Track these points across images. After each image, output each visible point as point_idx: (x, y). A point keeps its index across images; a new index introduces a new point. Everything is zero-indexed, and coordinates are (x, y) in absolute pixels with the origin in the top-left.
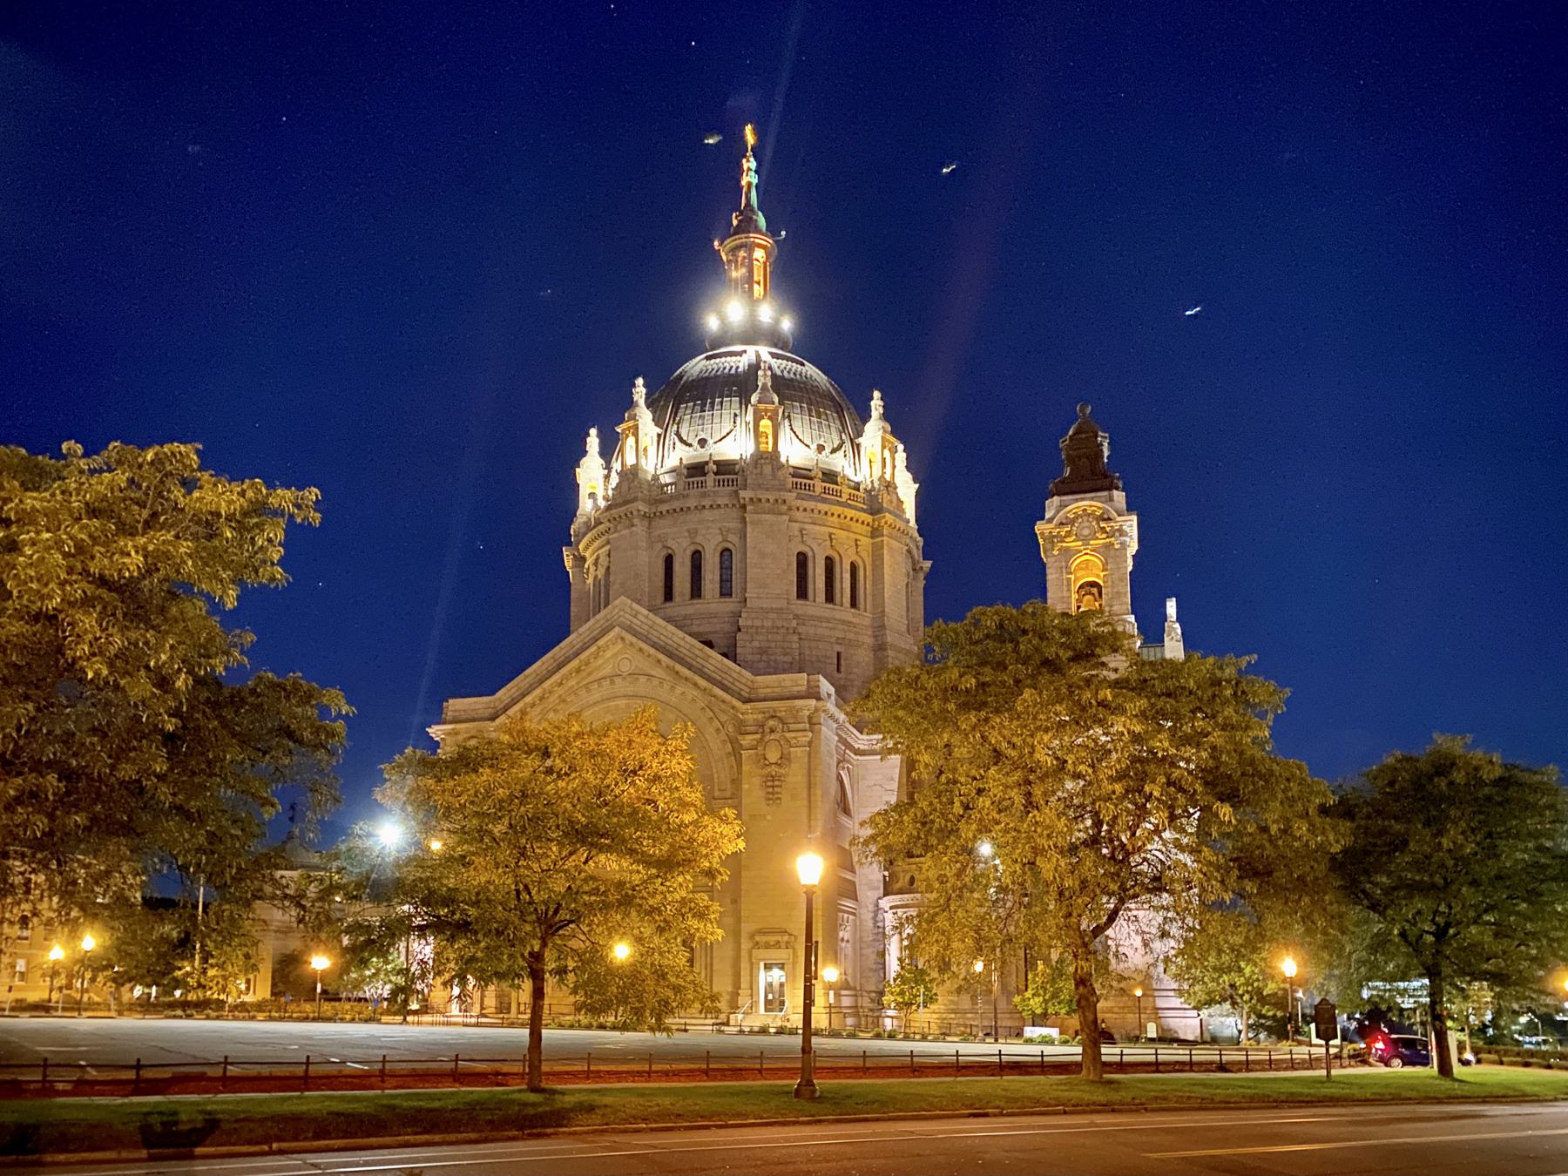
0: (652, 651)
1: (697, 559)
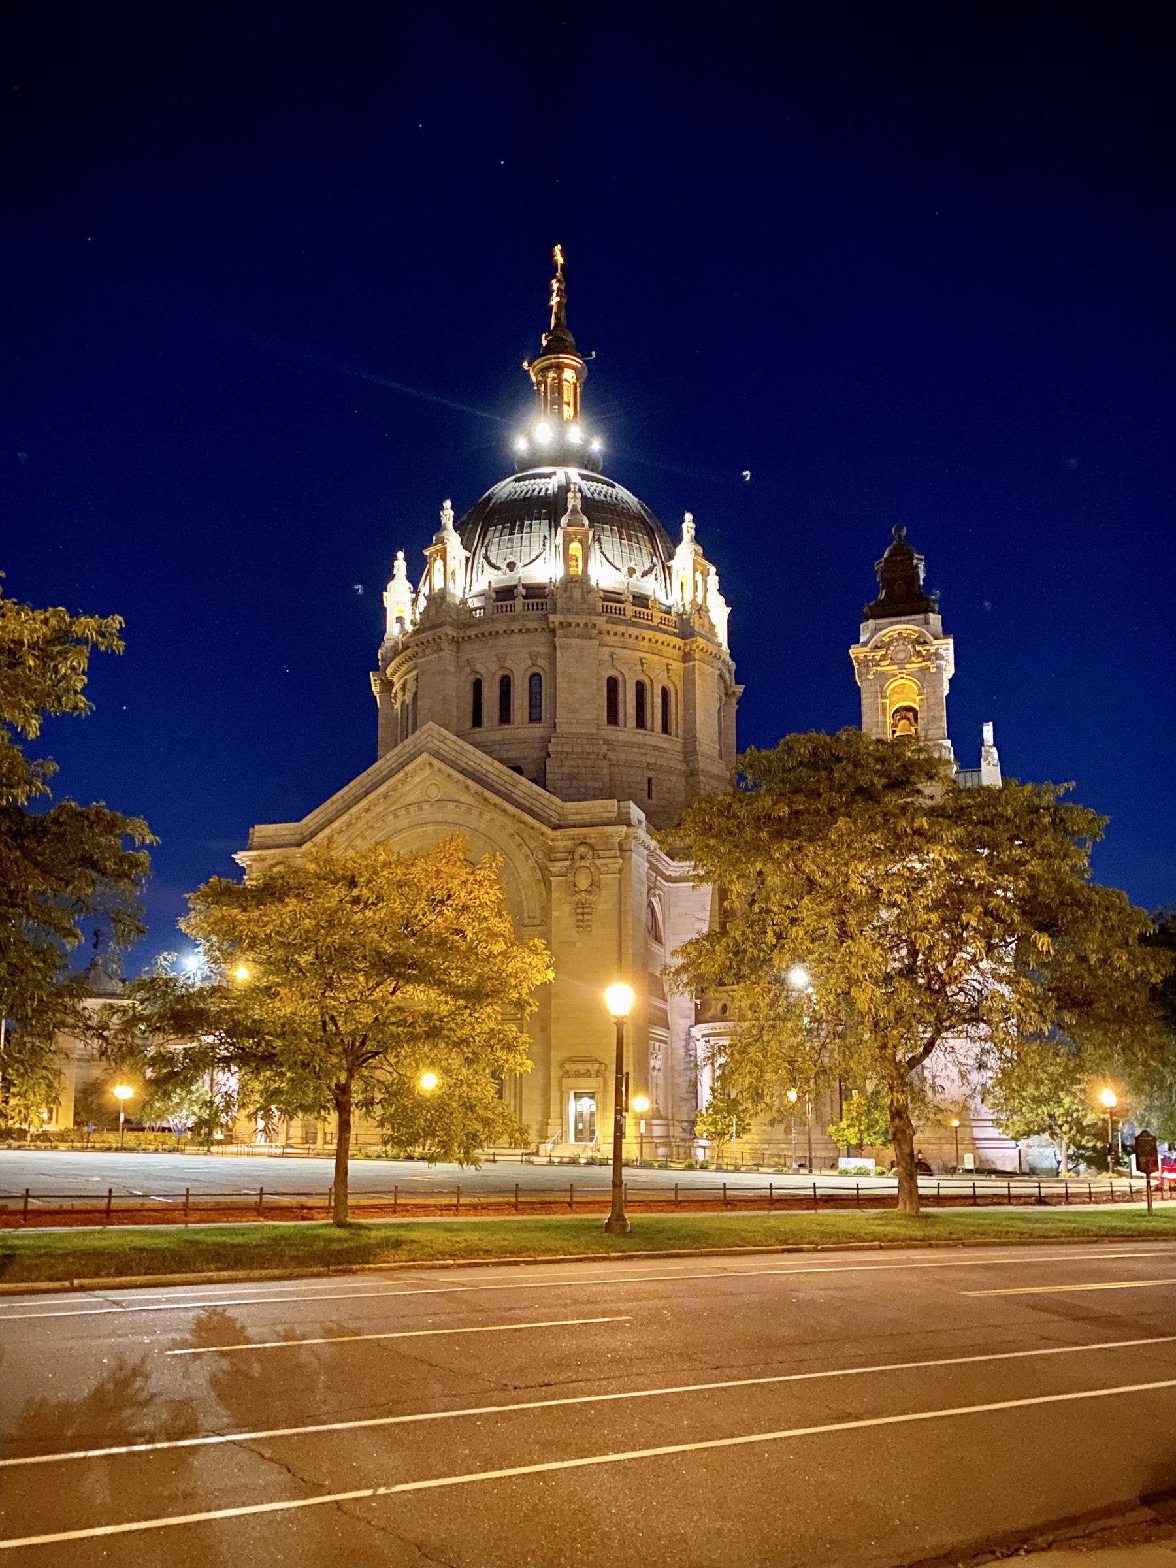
0: (460, 777)
1: (506, 683)
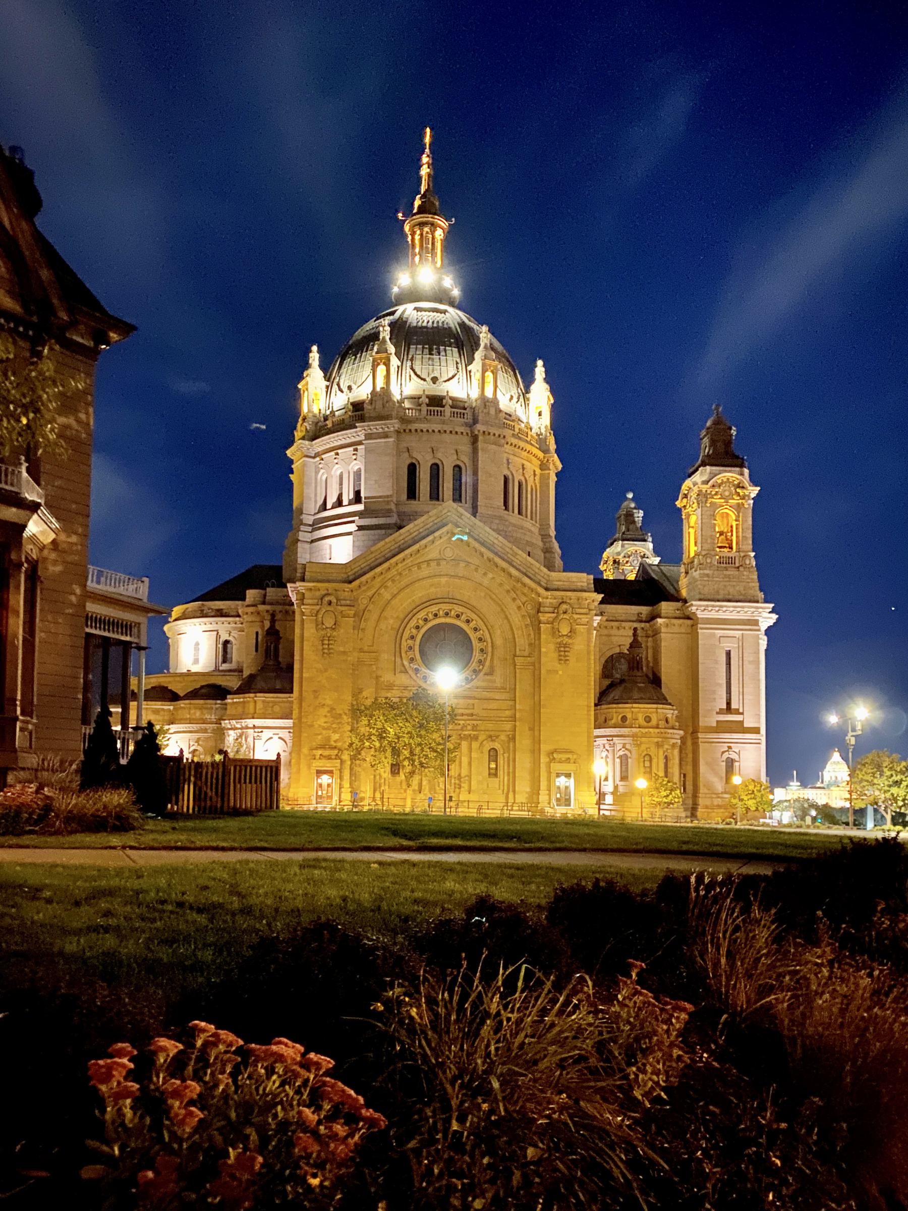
0: (477, 545)
1: (435, 470)
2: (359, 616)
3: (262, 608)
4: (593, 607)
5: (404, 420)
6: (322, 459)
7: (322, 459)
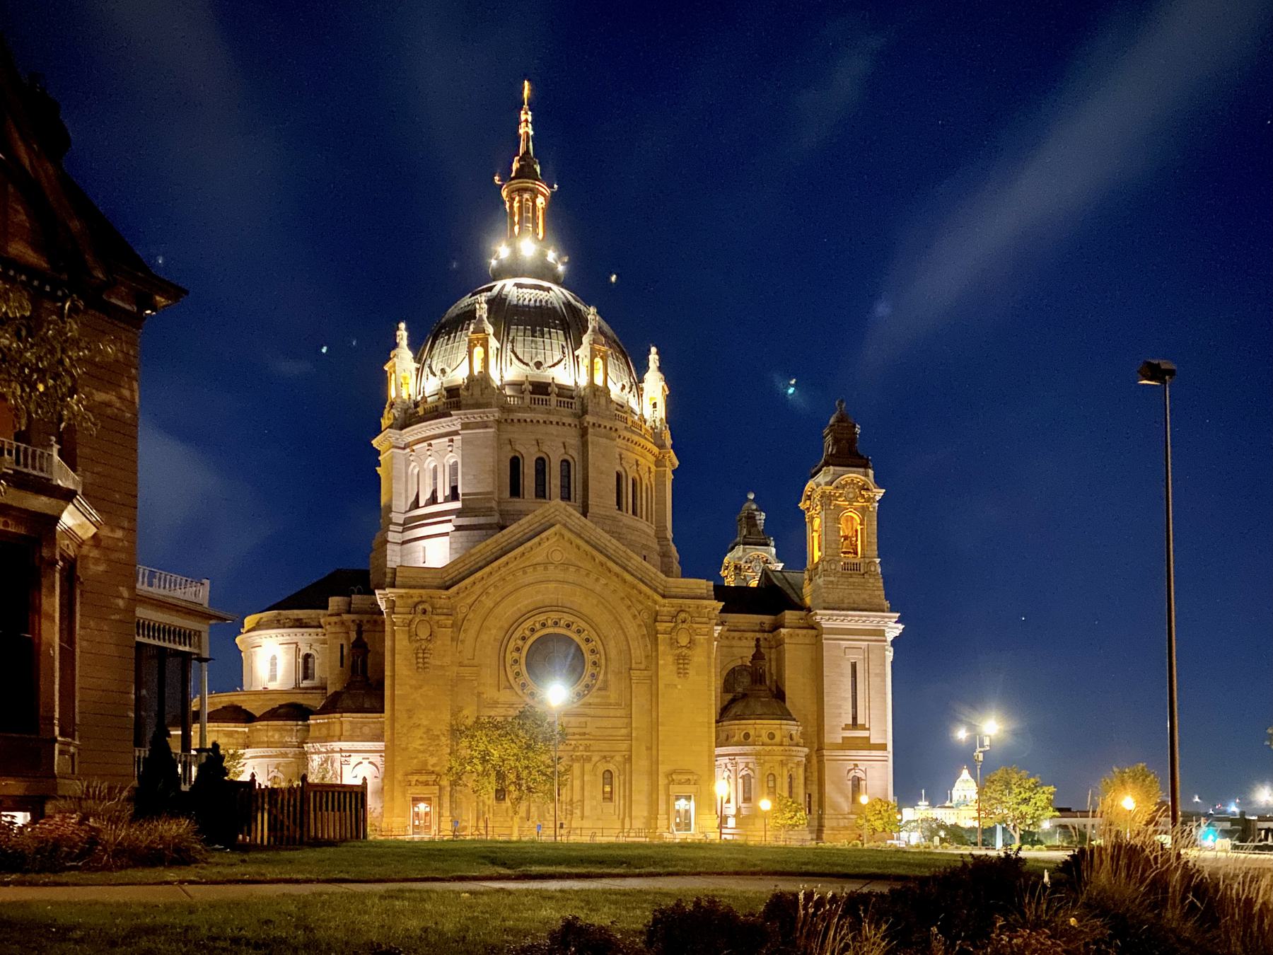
0: (588, 548)
2: (457, 626)
3: (345, 617)
4: (713, 616)
5: (505, 408)
6: (413, 451)
7: (413, 451)
